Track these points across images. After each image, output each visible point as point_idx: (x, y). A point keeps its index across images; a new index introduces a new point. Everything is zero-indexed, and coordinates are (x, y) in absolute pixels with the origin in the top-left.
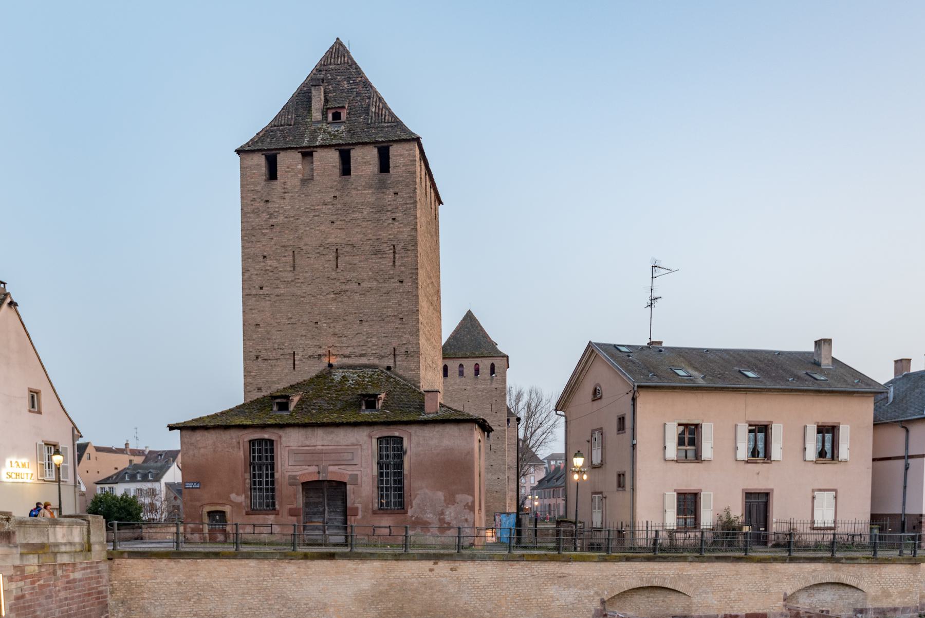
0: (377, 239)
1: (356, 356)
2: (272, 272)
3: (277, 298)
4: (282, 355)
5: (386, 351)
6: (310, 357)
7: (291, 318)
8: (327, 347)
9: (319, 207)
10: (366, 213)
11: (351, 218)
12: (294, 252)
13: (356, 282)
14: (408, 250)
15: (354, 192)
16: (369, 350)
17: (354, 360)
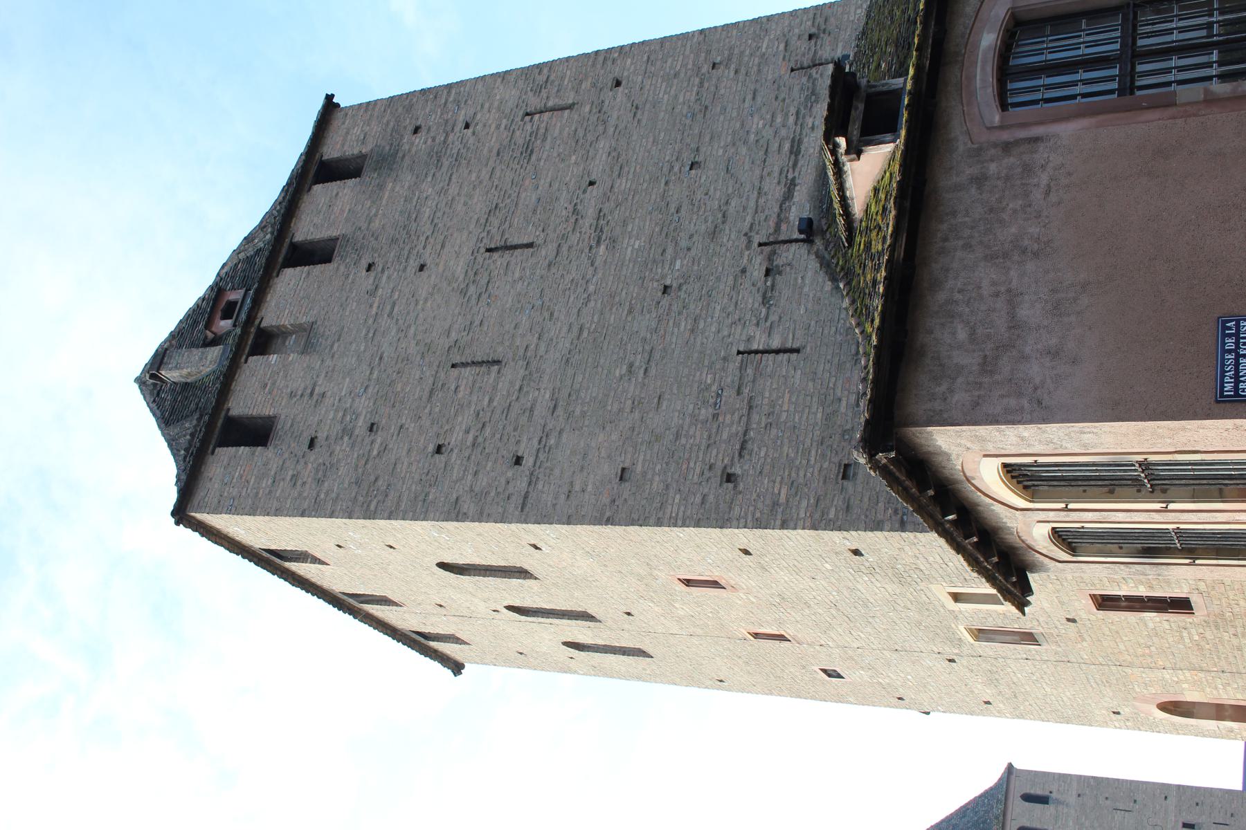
0: (498, 154)
1: (795, 165)
2: (484, 425)
3: (560, 411)
4: (739, 393)
5: (796, 89)
6: (765, 300)
7: (631, 365)
8: (747, 253)
9: (376, 305)
10: (430, 190)
11: (429, 222)
12: (453, 366)
13: (584, 192)
14: (547, 82)
15: (376, 224)
16: (783, 132)
17: (804, 169)
